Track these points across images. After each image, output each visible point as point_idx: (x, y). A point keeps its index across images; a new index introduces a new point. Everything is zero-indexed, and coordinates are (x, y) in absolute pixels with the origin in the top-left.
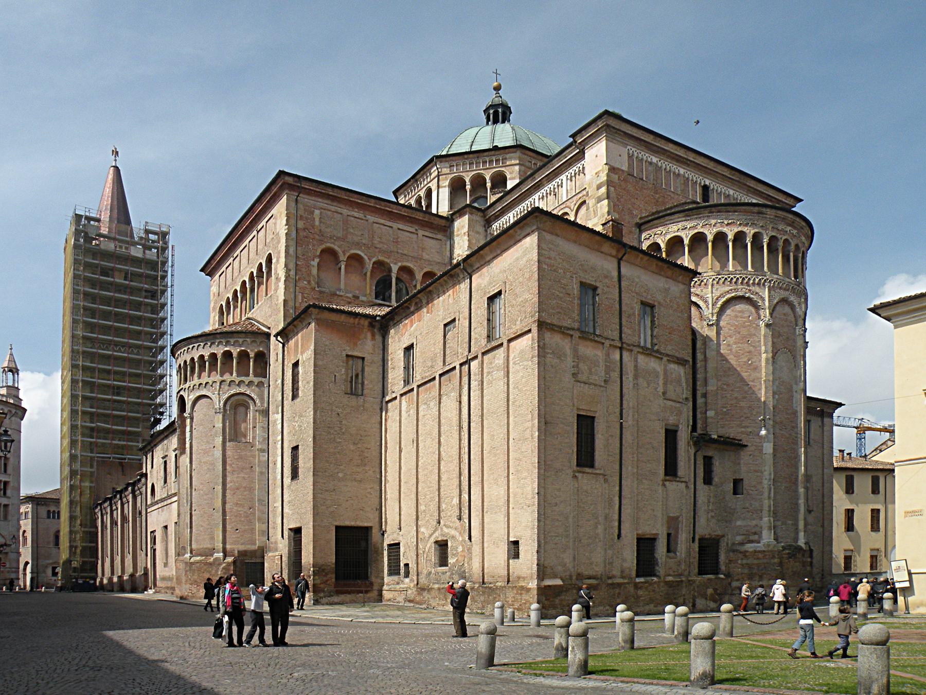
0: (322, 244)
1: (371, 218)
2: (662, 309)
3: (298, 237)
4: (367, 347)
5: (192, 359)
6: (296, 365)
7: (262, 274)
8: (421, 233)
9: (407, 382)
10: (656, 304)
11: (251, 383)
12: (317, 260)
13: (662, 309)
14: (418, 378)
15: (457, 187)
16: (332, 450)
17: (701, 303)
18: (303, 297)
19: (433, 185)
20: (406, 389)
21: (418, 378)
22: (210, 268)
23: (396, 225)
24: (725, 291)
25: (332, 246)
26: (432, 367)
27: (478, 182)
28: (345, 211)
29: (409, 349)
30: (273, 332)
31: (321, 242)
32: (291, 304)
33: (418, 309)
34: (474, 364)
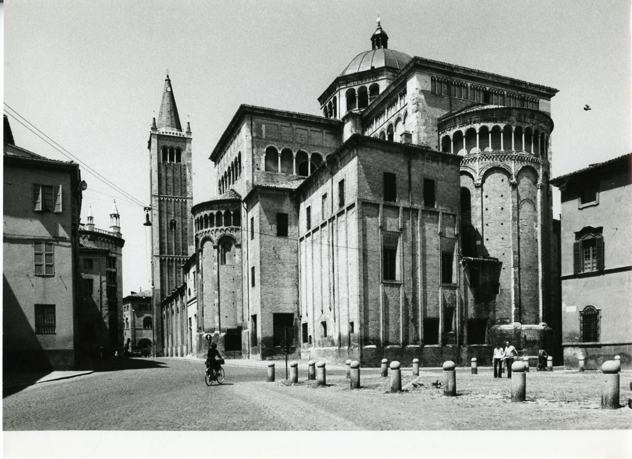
0: (266, 145)
1: (295, 126)
2: (439, 182)
3: (256, 142)
4: (287, 207)
5: (201, 216)
6: (252, 219)
7: (237, 165)
8: (325, 131)
9: (309, 227)
10: (435, 179)
11: (232, 229)
12: (265, 155)
13: (439, 182)
14: (313, 227)
15: (350, 97)
16: (270, 269)
17: (472, 173)
18: (257, 178)
19: (337, 95)
20: (308, 233)
21: (313, 227)
22: (216, 157)
23: (309, 129)
24: (488, 163)
25: (273, 145)
26: (318, 220)
27: (363, 90)
28: (280, 124)
29: (309, 209)
30: (243, 198)
31: (266, 144)
32: (251, 182)
33: (312, 186)
34: (335, 222)
